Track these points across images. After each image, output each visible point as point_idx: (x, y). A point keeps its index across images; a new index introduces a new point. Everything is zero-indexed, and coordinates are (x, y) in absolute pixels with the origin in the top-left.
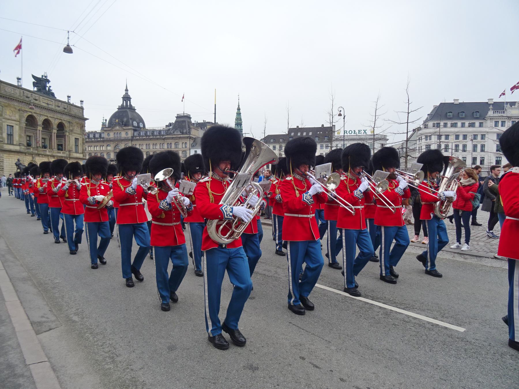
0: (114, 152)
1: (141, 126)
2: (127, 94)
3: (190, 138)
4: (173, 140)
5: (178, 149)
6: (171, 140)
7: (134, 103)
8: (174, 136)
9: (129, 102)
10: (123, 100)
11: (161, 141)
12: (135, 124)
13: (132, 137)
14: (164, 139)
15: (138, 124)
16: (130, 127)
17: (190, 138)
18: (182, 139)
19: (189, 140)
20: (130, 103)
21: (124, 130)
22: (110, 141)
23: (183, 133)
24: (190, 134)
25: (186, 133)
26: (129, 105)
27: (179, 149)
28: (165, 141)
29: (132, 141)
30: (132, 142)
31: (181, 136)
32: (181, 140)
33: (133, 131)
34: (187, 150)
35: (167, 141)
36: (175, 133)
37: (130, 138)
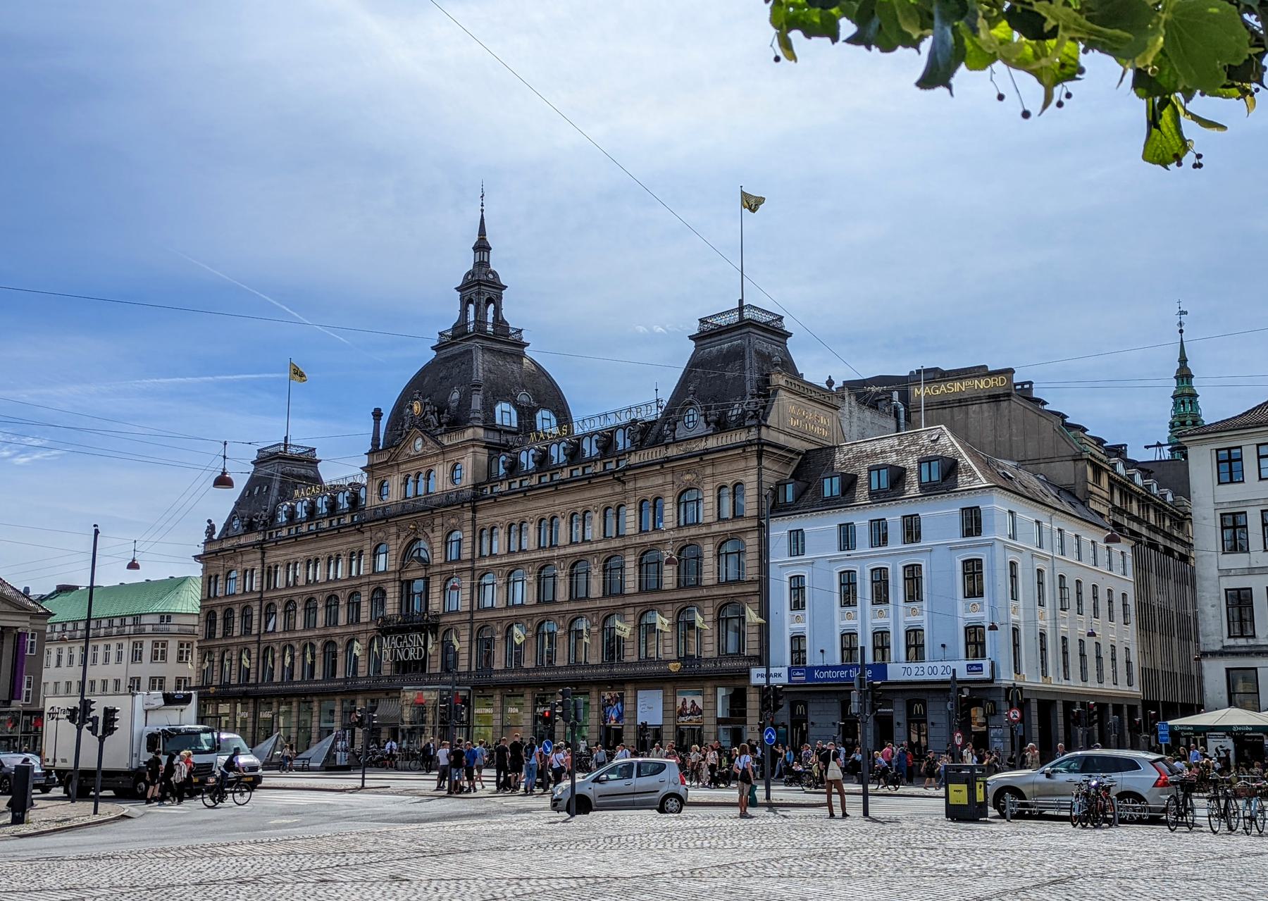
0: (402, 582)
1: (545, 420)
2: (482, 264)
3: (762, 449)
4: (669, 478)
5: (693, 531)
6: (659, 480)
7: (513, 311)
8: (673, 451)
9: (491, 307)
10: (462, 298)
11: (608, 491)
12: (505, 414)
13: (475, 486)
14: (619, 477)
15: (526, 414)
16: (469, 434)
17: (762, 449)
18: (713, 463)
19: (754, 462)
20: (497, 311)
21: (444, 450)
22: (385, 517)
23: (721, 426)
24: (759, 426)
25: (740, 425)
26: (490, 318)
27: (704, 530)
28: (630, 486)
29: (474, 510)
30: (477, 515)
31: (712, 443)
32: (709, 471)
33: (483, 456)
34: (744, 531)
35: (640, 484)
36: (681, 433)
37: (468, 493)
